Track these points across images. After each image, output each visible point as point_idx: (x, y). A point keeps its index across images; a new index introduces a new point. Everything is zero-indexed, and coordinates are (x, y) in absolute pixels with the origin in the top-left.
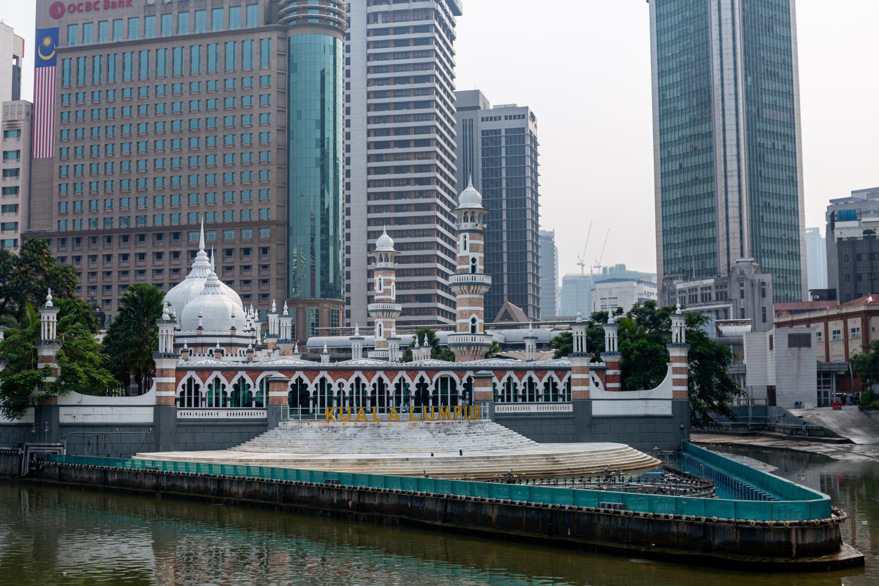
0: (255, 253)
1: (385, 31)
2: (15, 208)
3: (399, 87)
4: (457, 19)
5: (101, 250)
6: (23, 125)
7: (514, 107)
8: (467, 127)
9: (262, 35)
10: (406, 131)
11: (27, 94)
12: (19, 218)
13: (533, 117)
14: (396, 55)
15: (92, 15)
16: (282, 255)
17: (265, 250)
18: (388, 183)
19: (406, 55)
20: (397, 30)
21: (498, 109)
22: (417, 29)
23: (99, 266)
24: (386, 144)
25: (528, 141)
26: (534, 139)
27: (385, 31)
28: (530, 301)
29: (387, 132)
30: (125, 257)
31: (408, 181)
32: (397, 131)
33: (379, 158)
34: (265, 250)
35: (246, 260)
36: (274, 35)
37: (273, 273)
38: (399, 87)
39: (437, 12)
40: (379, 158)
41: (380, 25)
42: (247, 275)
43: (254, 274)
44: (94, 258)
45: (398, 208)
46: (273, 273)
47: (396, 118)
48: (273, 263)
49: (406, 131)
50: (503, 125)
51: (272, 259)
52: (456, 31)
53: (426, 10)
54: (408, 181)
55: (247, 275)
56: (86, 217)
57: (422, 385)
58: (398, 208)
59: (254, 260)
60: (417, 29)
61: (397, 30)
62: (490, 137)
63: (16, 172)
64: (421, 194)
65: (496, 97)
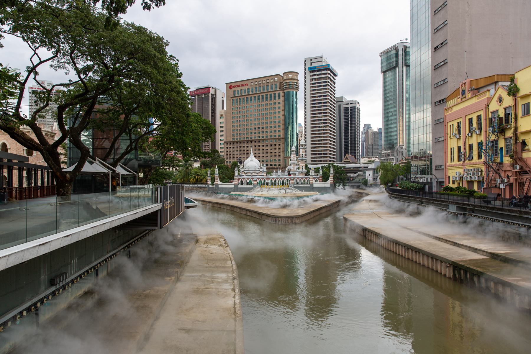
0: (277, 145)
1: (315, 83)
2: (223, 135)
3: (319, 98)
4: (336, 78)
5: (242, 145)
6: (224, 116)
7: (353, 101)
8: (340, 106)
9: (279, 92)
10: (321, 110)
11: (225, 109)
12: (224, 138)
13: (358, 103)
14: (318, 90)
15: (239, 88)
16: (283, 146)
17: (279, 145)
18: (316, 124)
19: (321, 90)
20: (319, 83)
21: (349, 101)
22: (324, 82)
23: (242, 149)
24: (315, 114)
25: (356, 110)
26: (359, 109)
27: (315, 83)
28: (357, 154)
29: (315, 110)
30: (248, 147)
31: (321, 123)
32: (318, 110)
33: (314, 117)
34: (279, 145)
35: (275, 147)
36: (281, 92)
37: (281, 150)
38: (319, 98)
39: (329, 78)
40: (314, 117)
41: (314, 82)
42: (275, 151)
43: (277, 151)
44: (241, 147)
45: (319, 130)
46: (281, 150)
47: (318, 107)
48: (281, 148)
49: (321, 110)
50: (349, 106)
51: (281, 147)
52: (335, 81)
53: (326, 77)
54: (321, 123)
55: (275, 151)
56: (239, 137)
57: (283, 181)
58: (319, 130)
59: (277, 147)
60: (324, 82)
61: (319, 83)
62: (346, 109)
63: (223, 127)
64: (325, 126)
65: (348, 98)
